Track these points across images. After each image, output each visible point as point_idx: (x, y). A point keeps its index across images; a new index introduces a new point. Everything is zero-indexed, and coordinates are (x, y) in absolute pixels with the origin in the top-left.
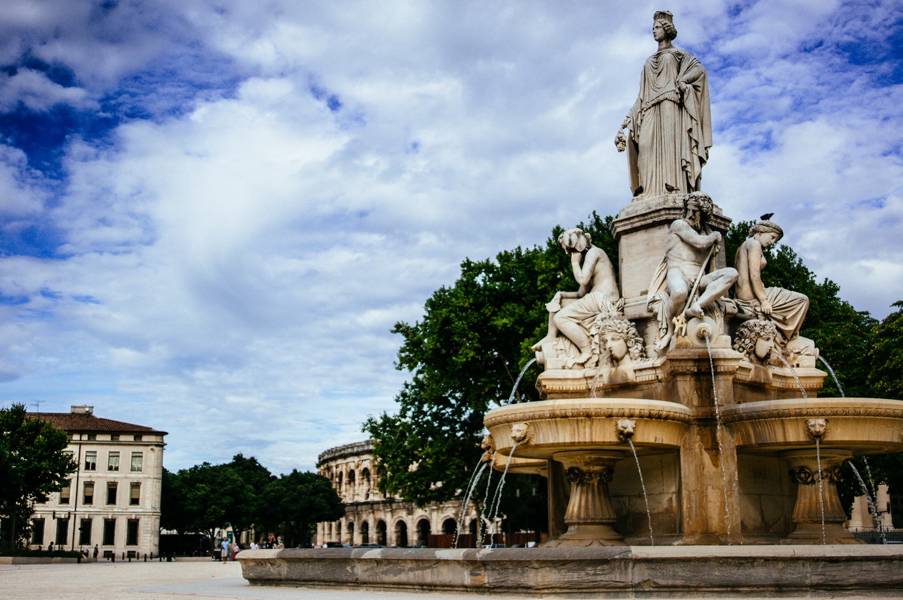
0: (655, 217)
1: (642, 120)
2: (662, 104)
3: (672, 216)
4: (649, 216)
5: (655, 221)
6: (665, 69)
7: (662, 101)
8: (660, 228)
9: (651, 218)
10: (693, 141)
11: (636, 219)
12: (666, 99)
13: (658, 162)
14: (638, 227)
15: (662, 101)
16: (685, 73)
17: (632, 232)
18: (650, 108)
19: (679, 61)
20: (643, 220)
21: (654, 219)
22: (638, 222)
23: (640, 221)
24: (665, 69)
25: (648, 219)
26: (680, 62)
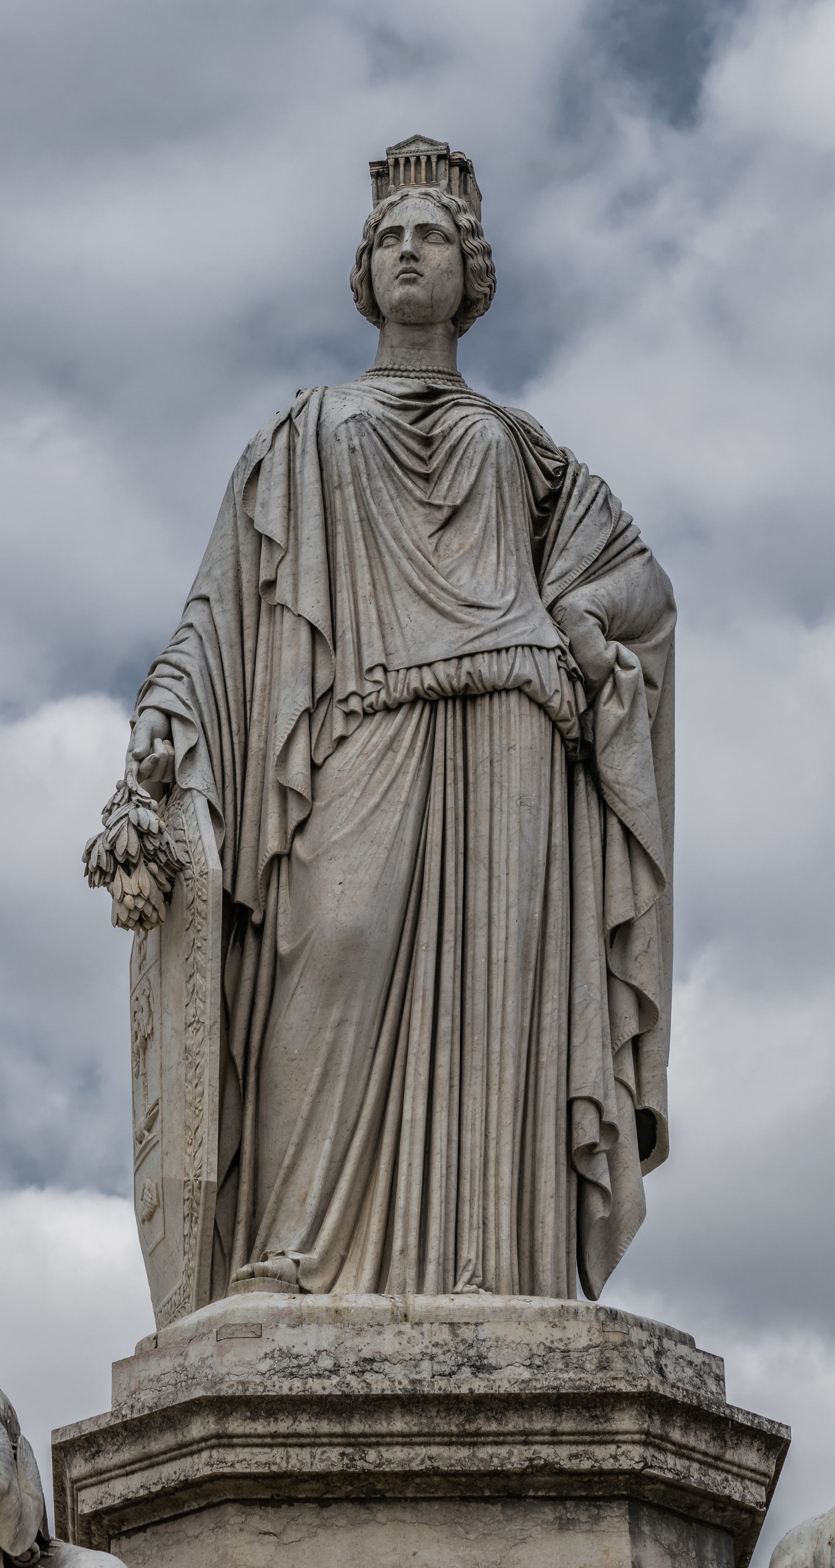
0: (555, 1438)
1: (315, 768)
2: (482, 711)
3: (671, 1461)
4: (514, 1423)
5: (550, 1469)
6: (488, 501)
7: (494, 692)
8: (564, 1525)
9: (527, 1438)
10: (626, 1005)
11: (399, 1425)
12: (521, 688)
13: (442, 1072)
14: (407, 1476)
15: (494, 692)
16: (589, 575)
17: (323, 1503)
18: (390, 709)
19: (543, 485)
20: (451, 1439)
21: (546, 1453)
22: (406, 1440)
23: (428, 1438)
24: (488, 501)
25: (499, 1439)
26: (554, 496)
